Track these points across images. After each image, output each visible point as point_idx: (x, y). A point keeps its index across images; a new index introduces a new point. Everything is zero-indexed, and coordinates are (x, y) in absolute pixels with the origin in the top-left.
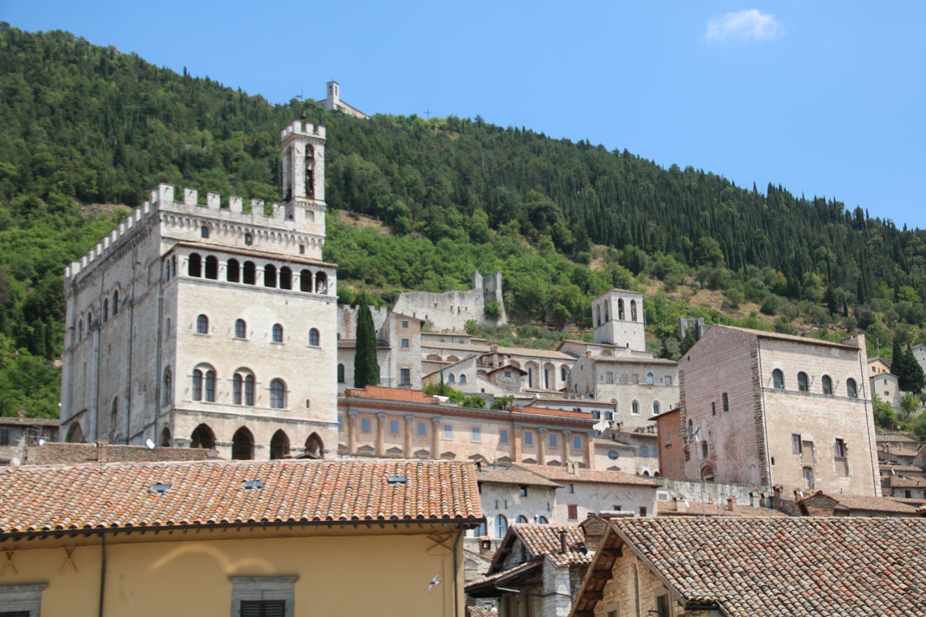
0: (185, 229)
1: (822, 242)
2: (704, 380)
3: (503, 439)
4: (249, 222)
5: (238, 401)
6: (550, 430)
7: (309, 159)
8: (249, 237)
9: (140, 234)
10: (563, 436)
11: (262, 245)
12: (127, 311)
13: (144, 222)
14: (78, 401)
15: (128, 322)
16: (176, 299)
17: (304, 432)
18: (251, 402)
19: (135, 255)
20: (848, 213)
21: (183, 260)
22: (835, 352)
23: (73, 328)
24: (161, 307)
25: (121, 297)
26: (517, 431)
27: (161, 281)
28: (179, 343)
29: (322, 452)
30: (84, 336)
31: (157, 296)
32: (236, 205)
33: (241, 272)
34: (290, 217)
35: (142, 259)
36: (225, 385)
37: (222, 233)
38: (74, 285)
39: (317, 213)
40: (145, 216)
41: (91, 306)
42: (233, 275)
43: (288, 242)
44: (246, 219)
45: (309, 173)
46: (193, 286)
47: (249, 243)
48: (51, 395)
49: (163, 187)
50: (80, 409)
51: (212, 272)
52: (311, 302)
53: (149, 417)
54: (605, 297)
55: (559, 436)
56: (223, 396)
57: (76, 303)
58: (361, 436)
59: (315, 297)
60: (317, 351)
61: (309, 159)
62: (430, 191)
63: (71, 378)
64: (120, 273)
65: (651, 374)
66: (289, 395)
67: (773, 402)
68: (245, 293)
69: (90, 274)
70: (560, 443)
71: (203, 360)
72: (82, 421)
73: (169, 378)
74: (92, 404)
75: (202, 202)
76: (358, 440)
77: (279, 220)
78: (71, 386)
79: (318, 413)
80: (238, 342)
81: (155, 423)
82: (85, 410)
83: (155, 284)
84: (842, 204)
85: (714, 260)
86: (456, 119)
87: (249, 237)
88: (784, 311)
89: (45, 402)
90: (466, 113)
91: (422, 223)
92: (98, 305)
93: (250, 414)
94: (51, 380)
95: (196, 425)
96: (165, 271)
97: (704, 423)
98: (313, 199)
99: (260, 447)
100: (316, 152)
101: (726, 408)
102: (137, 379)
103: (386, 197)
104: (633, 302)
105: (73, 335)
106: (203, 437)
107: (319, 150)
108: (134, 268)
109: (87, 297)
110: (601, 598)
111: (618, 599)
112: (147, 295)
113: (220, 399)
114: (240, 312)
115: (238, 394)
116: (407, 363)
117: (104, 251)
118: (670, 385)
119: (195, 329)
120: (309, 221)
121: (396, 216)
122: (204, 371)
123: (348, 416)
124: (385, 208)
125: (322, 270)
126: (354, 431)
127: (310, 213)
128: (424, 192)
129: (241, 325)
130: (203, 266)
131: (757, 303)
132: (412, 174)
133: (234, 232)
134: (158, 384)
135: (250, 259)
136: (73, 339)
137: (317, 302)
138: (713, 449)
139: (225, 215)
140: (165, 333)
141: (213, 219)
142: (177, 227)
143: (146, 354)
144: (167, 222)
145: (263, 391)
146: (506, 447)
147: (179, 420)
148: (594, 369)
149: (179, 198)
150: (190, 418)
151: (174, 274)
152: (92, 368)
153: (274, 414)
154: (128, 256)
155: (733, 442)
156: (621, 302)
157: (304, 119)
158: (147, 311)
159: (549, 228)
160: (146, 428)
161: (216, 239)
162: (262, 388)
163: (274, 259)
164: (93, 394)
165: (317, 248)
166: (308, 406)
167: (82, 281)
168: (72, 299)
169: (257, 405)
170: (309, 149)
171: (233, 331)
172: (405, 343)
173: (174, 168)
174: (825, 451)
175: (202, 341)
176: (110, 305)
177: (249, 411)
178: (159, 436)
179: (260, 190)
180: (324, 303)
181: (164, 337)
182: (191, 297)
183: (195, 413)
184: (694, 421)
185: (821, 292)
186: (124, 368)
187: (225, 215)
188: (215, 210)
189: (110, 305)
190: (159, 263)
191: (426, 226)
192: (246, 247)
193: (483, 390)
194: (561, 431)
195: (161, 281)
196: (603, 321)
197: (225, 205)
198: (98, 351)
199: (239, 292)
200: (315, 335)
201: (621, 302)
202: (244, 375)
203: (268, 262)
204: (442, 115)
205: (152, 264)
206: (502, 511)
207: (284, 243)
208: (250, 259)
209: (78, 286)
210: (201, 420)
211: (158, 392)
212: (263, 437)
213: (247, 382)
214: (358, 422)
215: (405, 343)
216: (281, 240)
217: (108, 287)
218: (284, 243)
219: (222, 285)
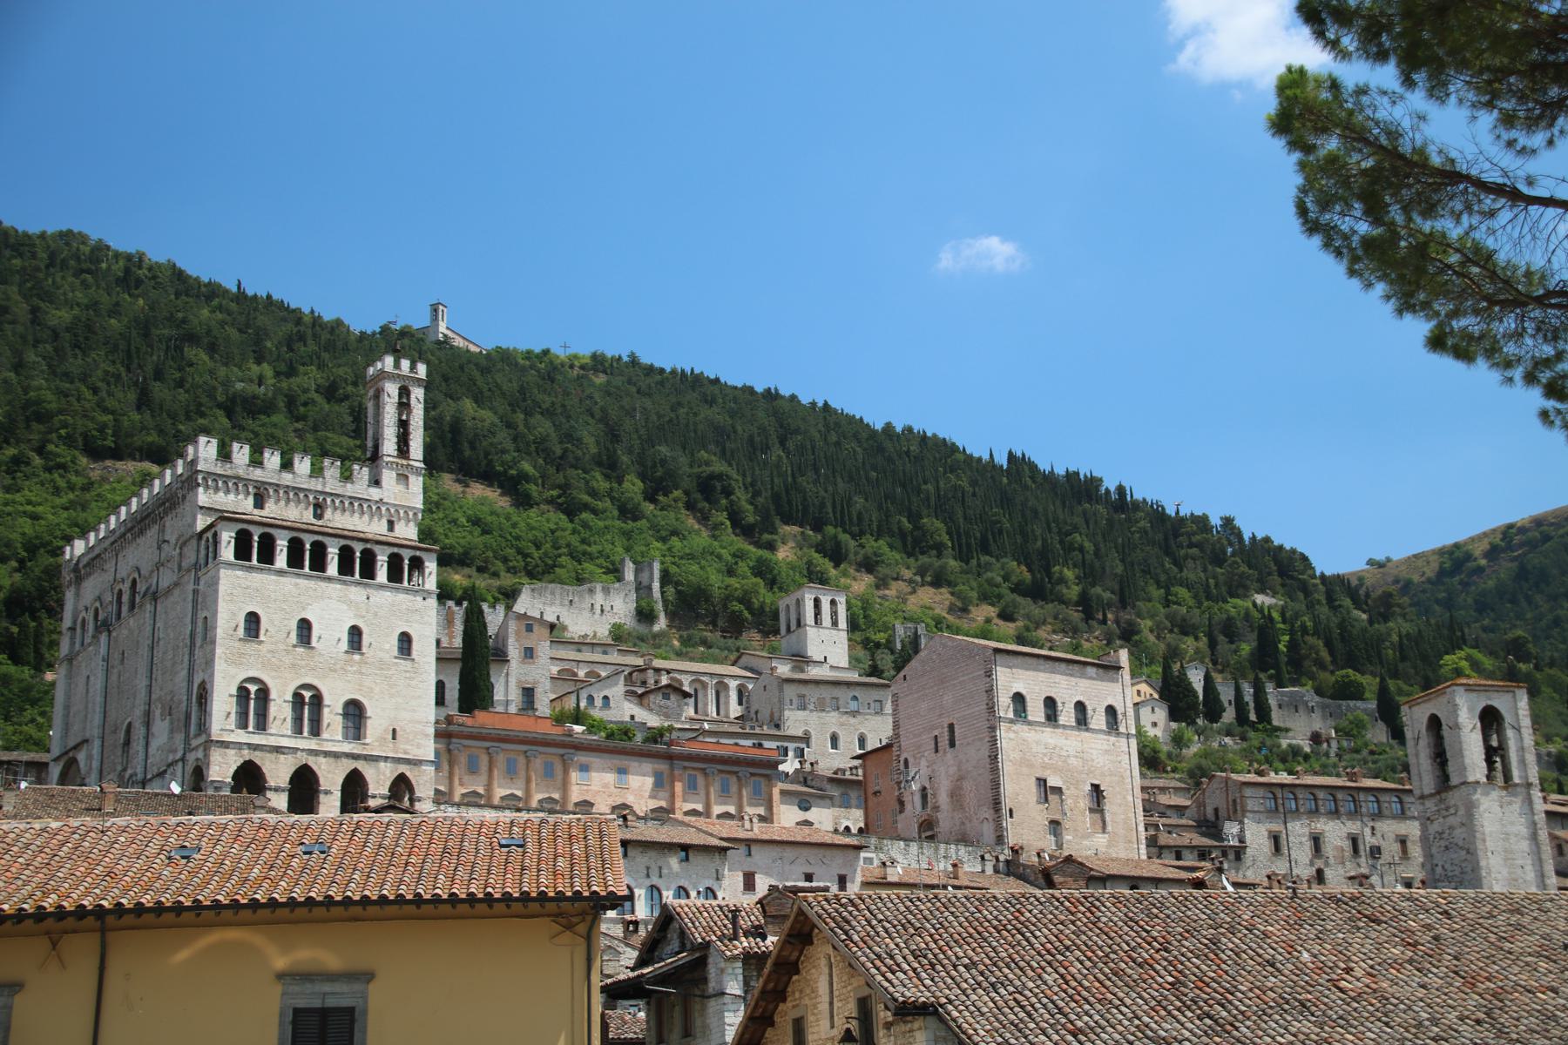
0: (232, 496)
1: (1076, 528)
2: (924, 706)
3: (658, 784)
4: (319, 488)
5: (298, 730)
6: (721, 771)
7: (404, 406)
8: (319, 510)
9: (171, 502)
10: (739, 779)
11: (336, 519)
12: (149, 607)
13: (175, 486)
14: (76, 728)
15: (149, 621)
16: (216, 591)
18: (316, 731)
19: (162, 530)
20: (1107, 491)
21: (227, 537)
22: (1091, 671)
23: (72, 629)
24: (195, 602)
25: (141, 587)
26: (676, 772)
27: (196, 567)
28: (219, 651)
29: (412, 800)
30: (88, 640)
31: (191, 587)
32: (303, 465)
33: (307, 555)
34: (376, 482)
35: (171, 536)
36: (280, 709)
37: (282, 503)
38: (76, 569)
39: (412, 478)
40: (176, 477)
41: (99, 598)
42: (295, 560)
43: (372, 516)
44: (316, 485)
45: (403, 426)
47: (318, 516)
48: (40, 720)
49: (202, 440)
50: (79, 740)
51: (267, 556)
52: (402, 596)
53: (175, 751)
54: (798, 594)
55: (734, 779)
56: (277, 722)
57: (77, 595)
58: (466, 778)
59: (407, 591)
60: (408, 663)
61: (404, 406)
62: (566, 450)
63: (68, 696)
64: (141, 554)
65: (855, 698)
66: (369, 722)
67: (1012, 735)
68: (312, 584)
69: (98, 556)
70: (734, 789)
71: (251, 674)
72: (81, 757)
73: (203, 697)
74: (96, 732)
75: (256, 462)
76: (461, 784)
77: (360, 486)
78: (67, 707)
80: (300, 650)
81: (183, 759)
82: (87, 741)
83: (189, 570)
84: (1101, 480)
85: (939, 548)
86: (603, 355)
87: (319, 510)
88: (1028, 617)
89: (30, 730)
90: (615, 348)
91: (555, 493)
92: (108, 597)
93: (314, 747)
94: (39, 700)
95: (240, 762)
96: (203, 552)
97: (924, 763)
98: (408, 458)
99: (327, 792)
100: (413, 397)
101: (952, 744)
102: (159, 699)
103: (507, 457)
104: (833, 602)
105: (72, 639)
106: (249, 778)
107: (418, 394)
108: (159, 548)
109: (92, 587)
110: (784, 1000)
111: (806, 1001)
112: (176, 584)
113: (273, 728)
115: (298, 720)
116: (530, 679)
117: (120, 524)
118: (880, 712)
119: (241, 632)
120: (401, 488)
121: (519, 483)
122: (253, 688)
123: (449, 751)
124: (505, 471)
125: (418, 553)
126: (457, 771)
127: (403, 478)
128: (559, 452)
129: (305, 627)
130: (255, 547)
131: (993, 605)
132: (543, 426)
133: (299, 501)
134: (189, 705)
135: (320, 538)
136: (73, 644)
137: (410, 597)
138: (934, 795)
139: (287, 479)
140: (201, 636)
142: (221, 494)
143: (174, 664)
144: (207, 487)
145: (332, 717)
146: (662, 794)
147: (216, 756)
148: (781, 690)
149: (225, 455)
150: (231, 752)
151: (215, 558)
152: (98, 684)
153: (347, 747)
154: (152, 533)
155: (961, 788)
156: (817, 602)
157: (398, 354)
158: (177, 607)
159: (724, 502)
160: (169, 765)
161: (272, 510)
163: (353, 538)
164: (97, 719)
165: (412, 524)
166: (394, 738)
167: (88, 564)
168: (73, 589)
169: (325, 735)
170: (404, 392)
172: (529, 653)
173: (220, 413)
174: (1077, 801)
175: (251, 647)
176: (125, 598)
177: (312, 744)
178: (187, 777)
179: (334, 445)
180: (419, 599)
181: (199, 642)
182: (238, 589)
183: (239, 746)
184: (911, 760)
185: (1073, 592)
186: (142, 683)
187: (287, 479)
188: (274, 471)
189: (125, 598)
190: (194, 542)
191: (559, 496)
192: (314, 521)
193: (632, 717)
194: (736, 773)
195: (196, 567)
196: (793, 627)
197: (287, 465)
198: (107, 660)
199: (302, 582)
200: (405, 641)
201: (817, 602)
202: (307, 694)
203: (343, 542)
204: (584, 348)
205: (184, 543)
206: (655, 880)
207: (366, 517)
208: (320, 538)
209: (81, 571)
210: (247, 755)
211: (188, 716)
212: (331, 778)
213: (310, 704)
214: (463, 759)
215: (529, 653)
216: (363, 513)
217: (122, 573)
218: (366, 517)
219: (281, 573)
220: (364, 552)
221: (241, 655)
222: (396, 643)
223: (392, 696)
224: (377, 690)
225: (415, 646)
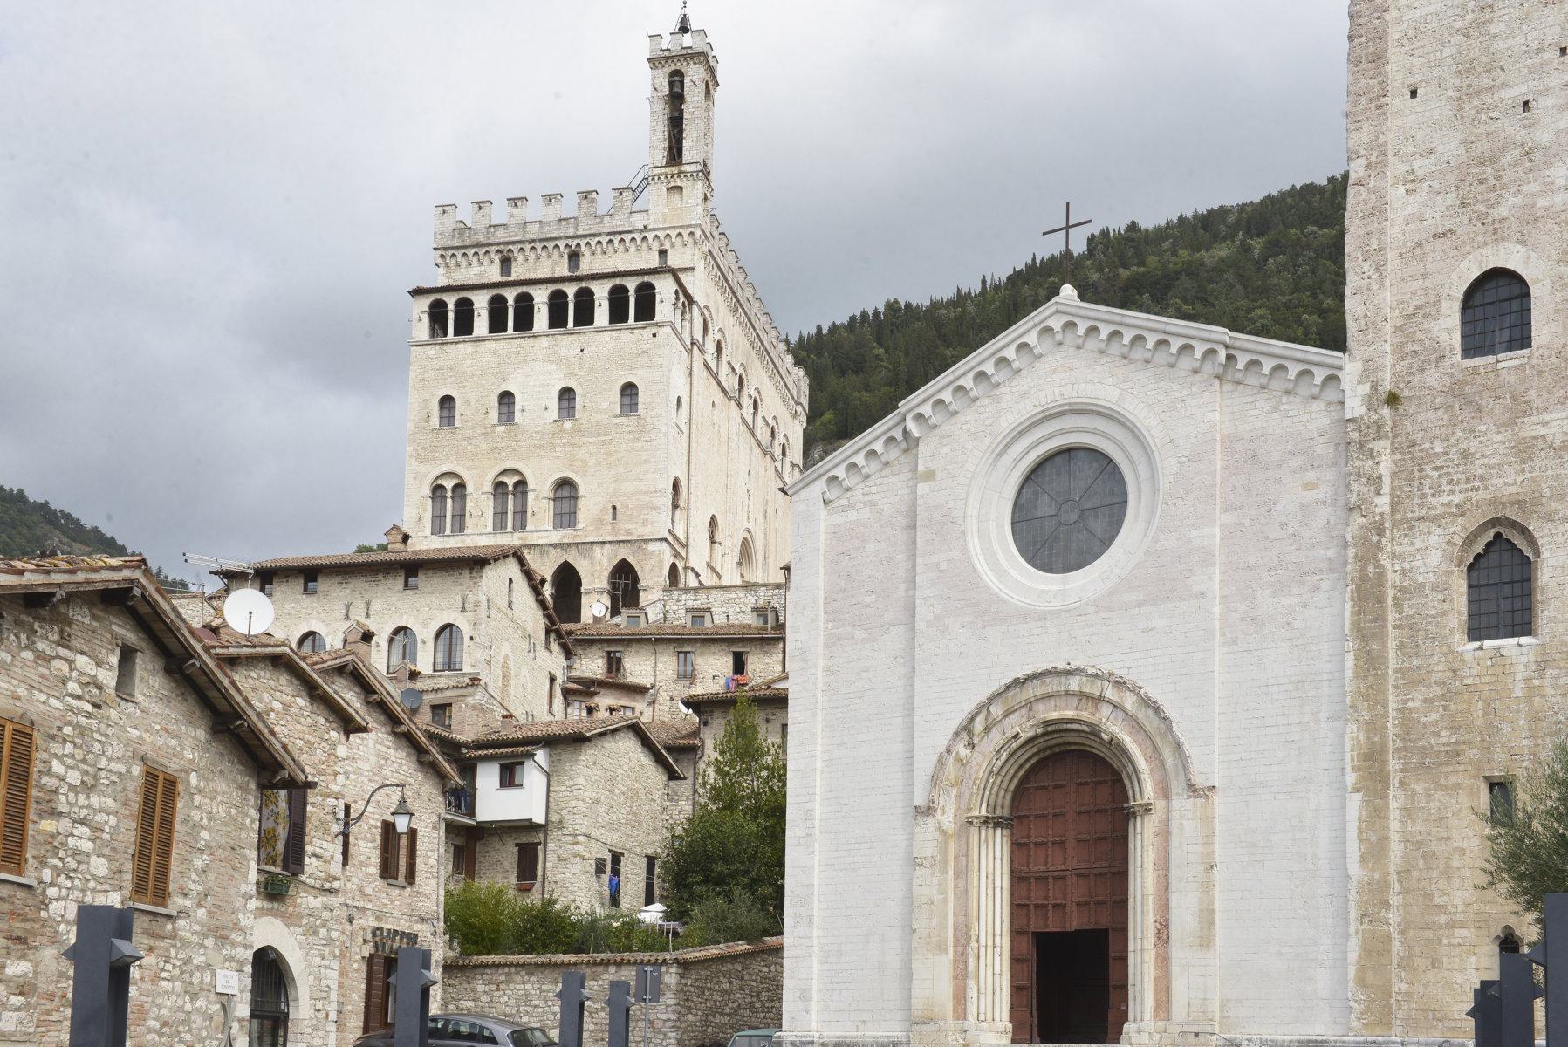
129: (506, 398)
141: (514, 243)
200: (629, 390)
203: (552, 287)
220: (579, 294)
224: (592, 462)
225: (641, 398)
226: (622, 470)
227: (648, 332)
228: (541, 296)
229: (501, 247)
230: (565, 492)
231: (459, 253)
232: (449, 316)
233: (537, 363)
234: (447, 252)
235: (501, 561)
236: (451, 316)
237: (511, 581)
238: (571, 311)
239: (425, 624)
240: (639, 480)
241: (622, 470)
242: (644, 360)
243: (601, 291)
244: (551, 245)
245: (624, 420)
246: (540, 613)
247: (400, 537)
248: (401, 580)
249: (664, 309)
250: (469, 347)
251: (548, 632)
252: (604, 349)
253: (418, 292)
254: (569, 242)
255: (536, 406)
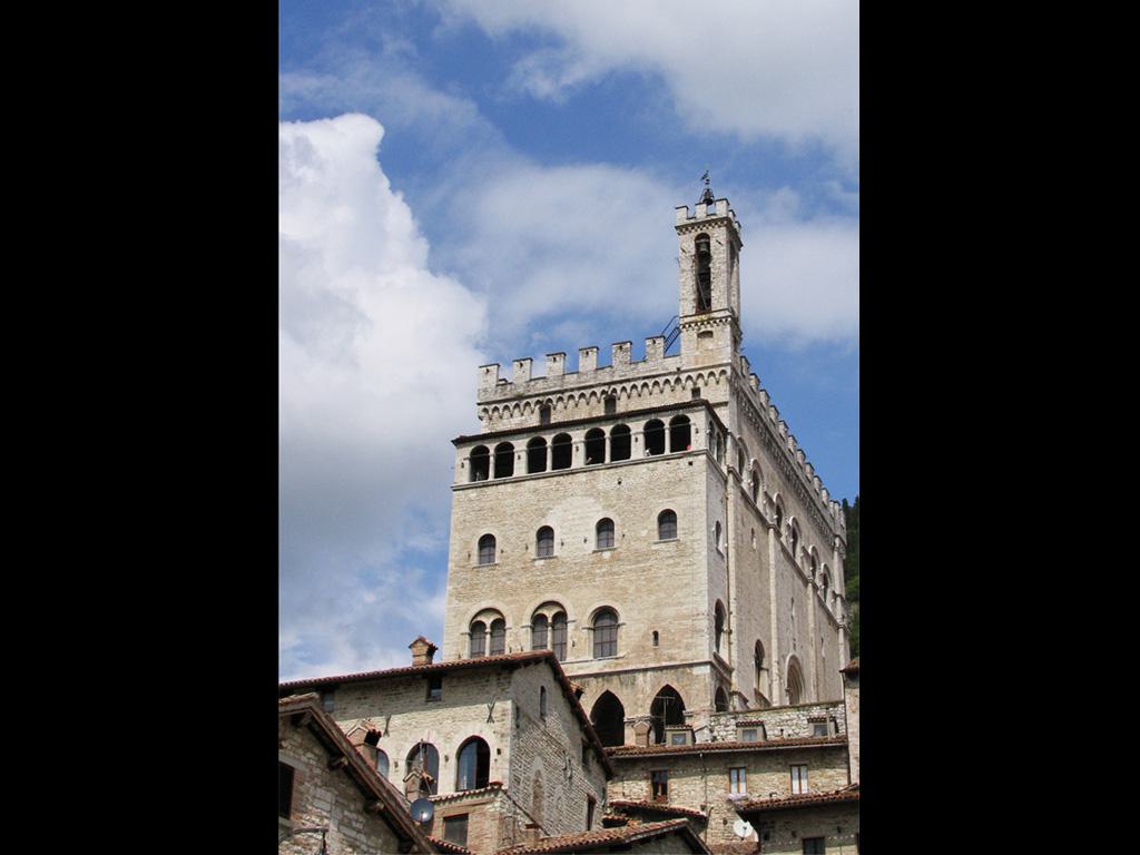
4: (608, 380)
17: (648, 689)
46: (473, 494)
66: (622, 632)
71: (484, 605)
79: (674, 651)
100: (713, 242)
107: (719, 236)
114: (544, 516)
119: (475, 559)
122: (488, 620)
125: (681, 412)
129: (545, 534)
153: (597, 666)
162: (576, 628)
170: (703, 242)
171: (533, 549)
200: (667, 518)
221: (473, 587)
222: (655, 525)
223: (650, 592)
226: (662, 595)
227: (685, 461)
228: (578, 437)
229: (540, 399)
230: (606, 622)
231: (501, 406)
232: (488, 460)
233: (573, 501)
234: (488, 407)
235: (532, 667)
236: (492, 459)
237: (543, 689)
238: (608, 445)
239: (448, 739)
240: (682, 604)
241: (662, 595)
242: (682, 488)
243: (637, 427)
244: (587, 392)
245: (663, 546)
246: (577, 727)
247: (425, 649)
248: (423, 692)
249: (699, 440)
250: (509, 488)
251: (585, 749)
252: (644, 482)
253: (460, 442)
254: (606, 388)
255: (575, 537)
